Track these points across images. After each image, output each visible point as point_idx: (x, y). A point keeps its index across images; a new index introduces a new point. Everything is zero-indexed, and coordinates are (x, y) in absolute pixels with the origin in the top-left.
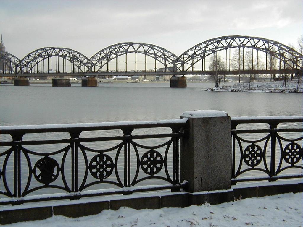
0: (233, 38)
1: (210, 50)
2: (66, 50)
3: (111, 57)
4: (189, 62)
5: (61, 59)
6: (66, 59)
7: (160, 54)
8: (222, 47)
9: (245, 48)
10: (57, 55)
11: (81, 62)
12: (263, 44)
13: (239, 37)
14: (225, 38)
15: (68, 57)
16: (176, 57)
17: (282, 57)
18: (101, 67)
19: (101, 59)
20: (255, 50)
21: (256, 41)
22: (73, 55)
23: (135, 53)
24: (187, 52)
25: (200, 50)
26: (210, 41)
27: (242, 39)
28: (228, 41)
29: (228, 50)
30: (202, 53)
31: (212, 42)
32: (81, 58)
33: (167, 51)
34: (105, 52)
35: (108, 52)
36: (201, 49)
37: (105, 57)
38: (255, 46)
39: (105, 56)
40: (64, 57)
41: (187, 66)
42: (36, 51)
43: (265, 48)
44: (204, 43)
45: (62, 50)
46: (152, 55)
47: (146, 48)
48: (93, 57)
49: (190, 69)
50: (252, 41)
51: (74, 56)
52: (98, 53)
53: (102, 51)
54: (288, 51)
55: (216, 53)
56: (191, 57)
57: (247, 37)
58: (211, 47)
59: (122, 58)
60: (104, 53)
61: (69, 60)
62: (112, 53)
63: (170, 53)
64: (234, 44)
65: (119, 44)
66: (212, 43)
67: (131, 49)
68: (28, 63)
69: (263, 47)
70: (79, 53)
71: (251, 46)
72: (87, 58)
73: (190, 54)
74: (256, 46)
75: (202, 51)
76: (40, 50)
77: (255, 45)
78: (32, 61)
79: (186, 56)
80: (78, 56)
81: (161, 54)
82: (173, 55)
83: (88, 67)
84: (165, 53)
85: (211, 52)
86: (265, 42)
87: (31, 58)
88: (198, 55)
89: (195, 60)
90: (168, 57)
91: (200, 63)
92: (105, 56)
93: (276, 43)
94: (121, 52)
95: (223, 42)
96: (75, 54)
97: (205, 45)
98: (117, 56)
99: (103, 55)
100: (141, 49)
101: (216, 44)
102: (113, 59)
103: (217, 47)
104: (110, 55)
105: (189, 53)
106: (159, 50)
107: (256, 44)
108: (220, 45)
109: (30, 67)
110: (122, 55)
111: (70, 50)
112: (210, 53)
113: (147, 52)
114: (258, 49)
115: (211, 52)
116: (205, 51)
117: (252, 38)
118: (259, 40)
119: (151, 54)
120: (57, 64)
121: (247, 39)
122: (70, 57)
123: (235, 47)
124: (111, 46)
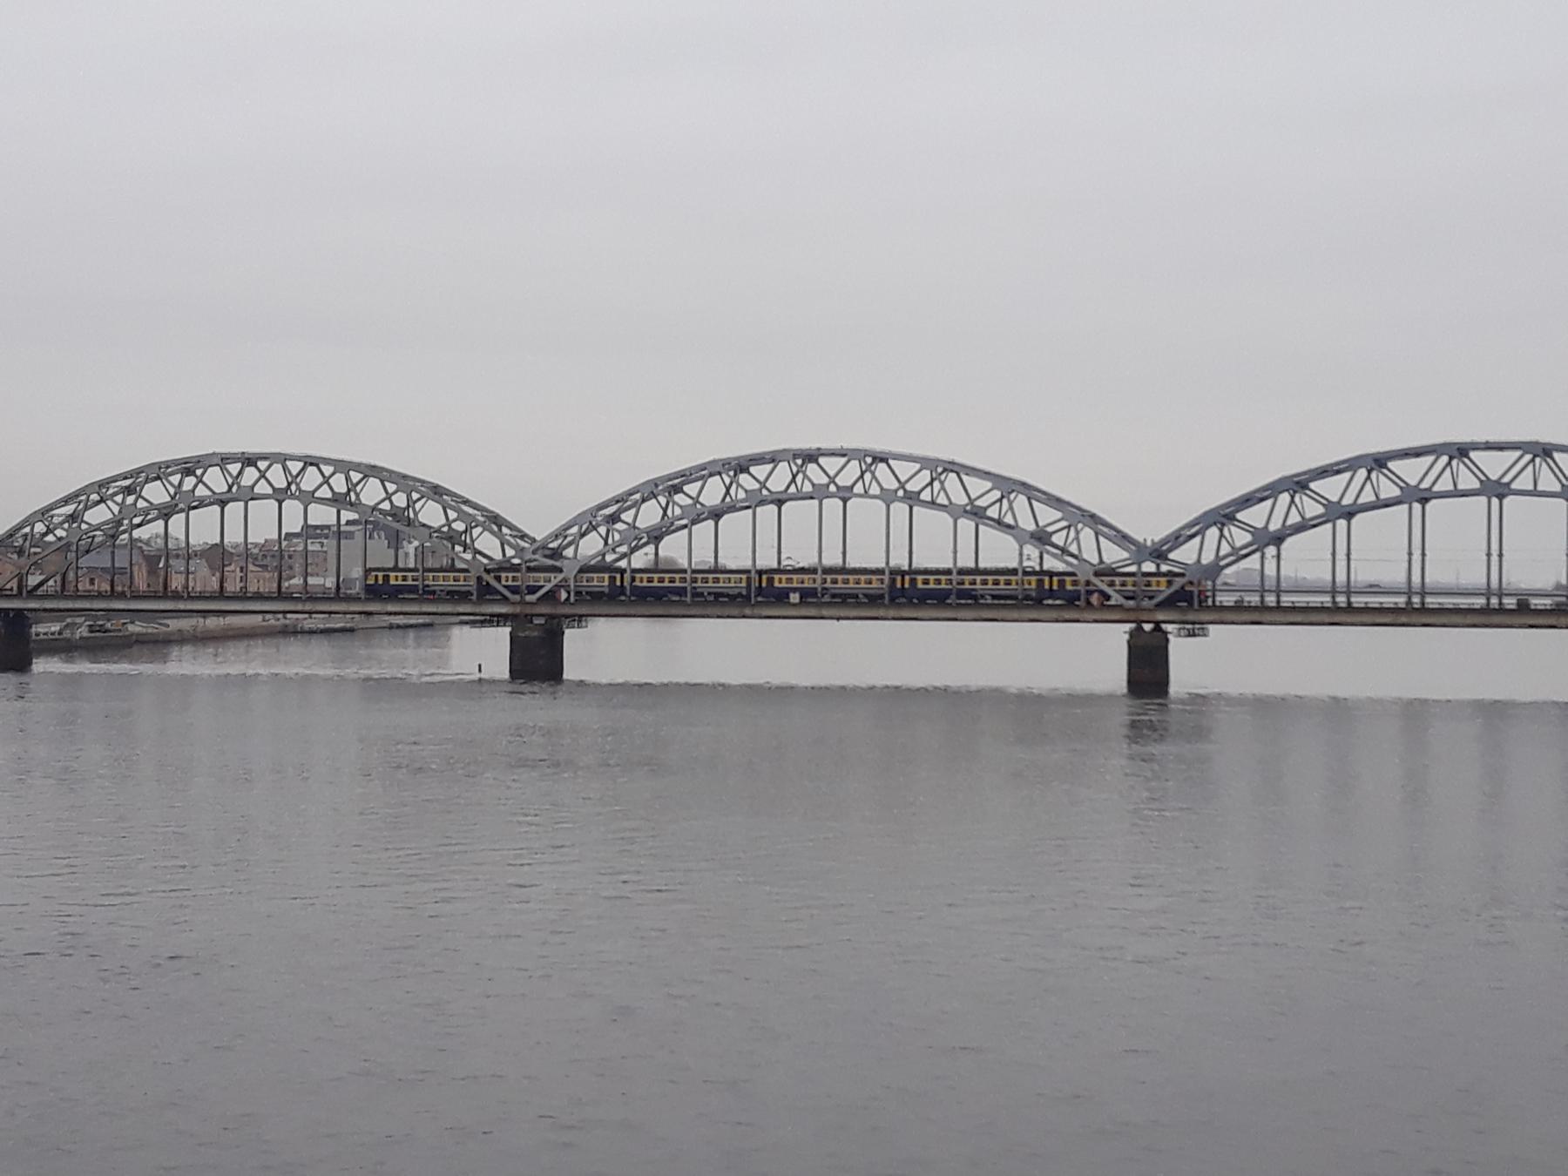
0: (249, 461)
12: (384, 495)
13: (283, 459)
21: (355, 476)
28: (234, 468)
57: (310, 462)
69: (386, 506)
71: (329, 495)
73: (56, 520)
74: (357, 495)
86: (391, 487)
93: (437, 492)
101: (175, 479)
107: (358, 488)
108: (201, 491)
112: (149, 517)
117: (343, 466)
121: (252, 469)
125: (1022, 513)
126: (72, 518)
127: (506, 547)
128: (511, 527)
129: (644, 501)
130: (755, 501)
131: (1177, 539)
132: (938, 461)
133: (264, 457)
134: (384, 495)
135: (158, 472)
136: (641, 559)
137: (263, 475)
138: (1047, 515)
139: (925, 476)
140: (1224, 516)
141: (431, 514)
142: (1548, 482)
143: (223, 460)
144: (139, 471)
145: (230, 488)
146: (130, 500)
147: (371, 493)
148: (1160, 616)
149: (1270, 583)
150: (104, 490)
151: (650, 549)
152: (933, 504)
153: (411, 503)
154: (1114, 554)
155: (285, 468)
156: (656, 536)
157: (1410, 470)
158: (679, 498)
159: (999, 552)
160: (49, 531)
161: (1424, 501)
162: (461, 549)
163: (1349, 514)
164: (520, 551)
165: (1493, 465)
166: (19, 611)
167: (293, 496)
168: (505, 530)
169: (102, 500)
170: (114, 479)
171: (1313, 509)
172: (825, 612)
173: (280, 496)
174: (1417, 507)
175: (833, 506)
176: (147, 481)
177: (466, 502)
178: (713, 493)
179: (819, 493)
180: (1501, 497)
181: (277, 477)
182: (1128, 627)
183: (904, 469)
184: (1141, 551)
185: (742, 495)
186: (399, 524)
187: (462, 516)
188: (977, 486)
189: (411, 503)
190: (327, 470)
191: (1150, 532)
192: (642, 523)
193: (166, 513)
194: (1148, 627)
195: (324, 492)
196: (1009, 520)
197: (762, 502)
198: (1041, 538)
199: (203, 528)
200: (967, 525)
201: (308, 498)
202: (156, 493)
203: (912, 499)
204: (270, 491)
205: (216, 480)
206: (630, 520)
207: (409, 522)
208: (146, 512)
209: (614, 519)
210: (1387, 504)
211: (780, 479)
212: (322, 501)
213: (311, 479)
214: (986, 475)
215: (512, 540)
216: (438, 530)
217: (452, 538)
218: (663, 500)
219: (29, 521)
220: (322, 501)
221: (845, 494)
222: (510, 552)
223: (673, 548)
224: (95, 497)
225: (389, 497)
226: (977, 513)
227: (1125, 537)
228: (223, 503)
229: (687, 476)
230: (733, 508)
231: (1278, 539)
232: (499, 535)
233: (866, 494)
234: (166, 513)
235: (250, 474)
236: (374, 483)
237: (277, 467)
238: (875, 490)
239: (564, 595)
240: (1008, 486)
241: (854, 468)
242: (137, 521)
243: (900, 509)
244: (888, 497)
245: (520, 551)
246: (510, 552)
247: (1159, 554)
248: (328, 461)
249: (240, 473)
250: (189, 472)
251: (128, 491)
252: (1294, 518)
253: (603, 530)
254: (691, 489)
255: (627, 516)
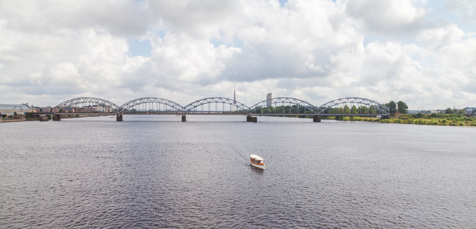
0: (86, 98)
1: (74, 103)
13: (90, 98)
21: (98, 100)
28: (84, 99)
57: (93, 98)
69: (102, 103)
86: (102, 101)
93: (108, 102)
101: (77, 100)
108: (80, 101)
117: (97, 99)
125: (171, 104)
126: (65, 104)
128: (116, 105)
129: (131, 103)
130: (143, 103)
131: (186, 107)
132: (162, 99)
133: (87, 98)
135: (75, 99)
136: (131, 109)
138: (174, 104)
139: (161, 100)
140: (191, 104)
141: (107, 104)
142: (221, 101)
143: (83, 98)
144: (73, 99)
146: (72, 102)
147: (100, 102)
148: (185, 114)
149: (195, 111)
151: (132, 107)
152: (162, 103)
153: (105, 103)
154: (180, 108)
156: (132, 106)
157: (209, 100)
158: (135, 102)
159: (169, 108)
160: (62, 106)
161: (210, 103)
163: (203, 104)
164: (117, 108)
165: (216, 100)
166: (59, 115)
169: (68, 102)
171: (200, 104)
172: (151, 114)
173: (90, 102)
174: (209, 103)
175: (151, 103)
176: (74, 100)
177: (111, 103)
178: (138, 102)
179: (150, 102)
180: (217, 103)
181: (89, 100)
182: (181, 116)
183: (159, 100)
184: (183, 108)
185: (142, 102)
186: (103, 106)
187: (111, 104)
188: (166, 101)
189: (105, 103)
190: (95, 99)
191: (184, 106)
192: (131, 105)
193: (76, 104)
194: (184, 115)
195: (95, 102)
196: (170, 105)
197: (144, 103)
198: (173, 106)
199: (81, 106)
200: (165, 105)
201: (93, 102)
202: (75, 102)
203: (160, 102)
204: (88, 101)
205: (82, 100)
207: (105, 105)
208: (74, 104)
209: (128, 104)
210: (206, 103)
211: (146, 100)
212: (94, 102)
213: (93, 100)
214: (167, 100)
217: (110, 106)
218: (133, 103)
219: (60, 105)
220: (94, 102)
221: (153, 102)
222: (116, 108)
223: (134, 107)
224: (67, 102)
226: (166, 104)
227: (181, 106)
228: (83, 103)
229: (136, 100)
230: (140, 103)
231: (196, 107)
233: (155, 102)
234: (76, 104)
235: (86, 100)
236: (100, 101)
237: (89, 99)
238: (156, 102)
239: (122, 112)
240: (169, 101)
241: (153, 99)
242: (73, 105)
243: (158, 104)
244: (157, 102)
245: (117, 108)
246: (116, 108)
247: (185, 108)
248: (95, 98)
250: (79, 99)
251: (72, 101)
252: (198, 105)
253: (126, 106)
254: (136, 101)
255: (129, 104)
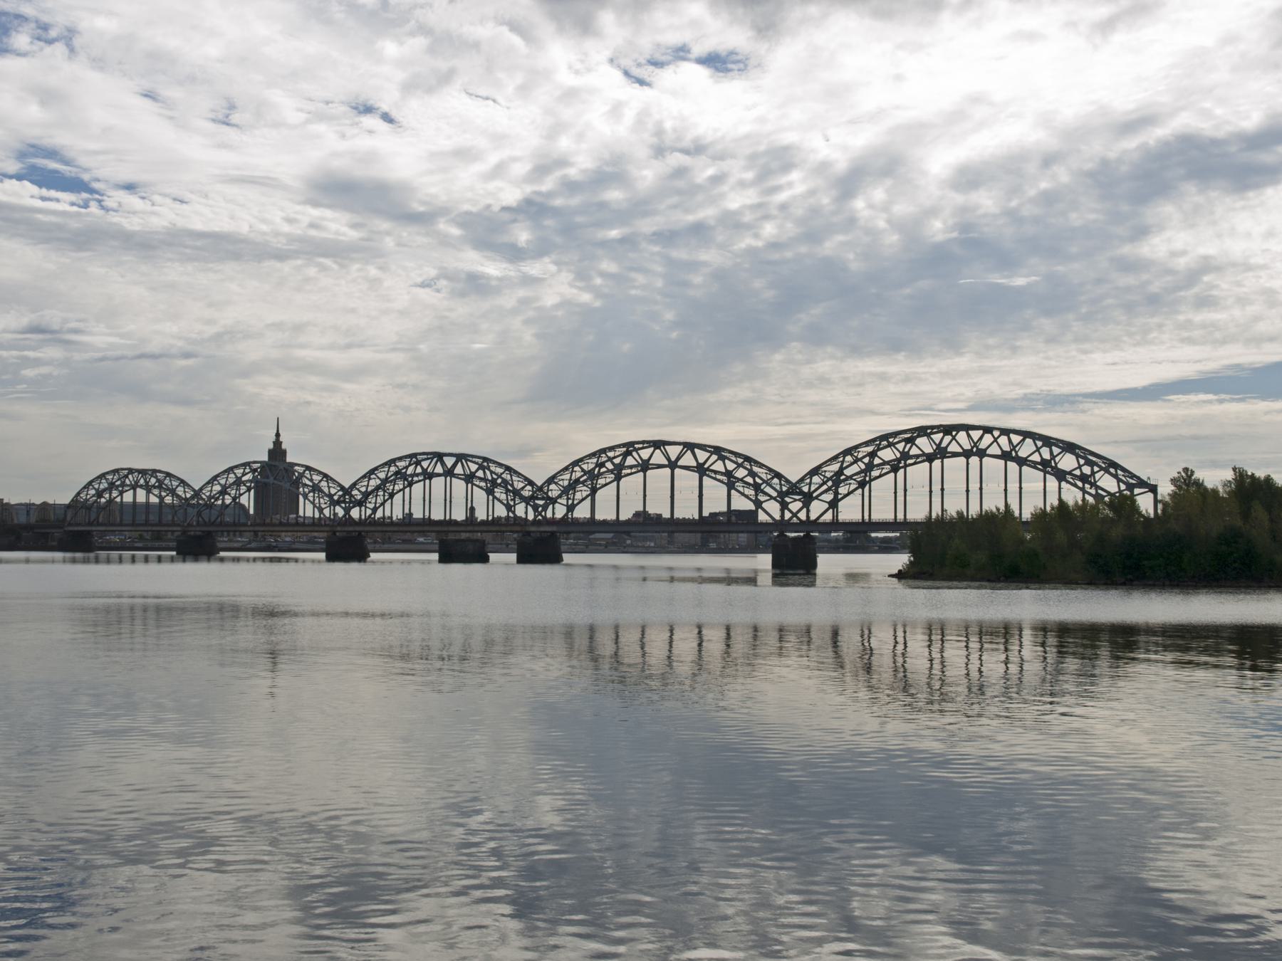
0: (948, 430)
1: (885, 463)
2: (474, 460)
3: (601, 481)
4: (824, 497)
5: (459, 486)
6: (473, 484)
7: (741, 473)
8: (917, 456)
9: (985, 460)
10: (449, 473)
11: (516, 493)
12: (1035, 449)
13: (967, 428)
14: (929, 431)
15: (481, 479)
16: (787, 481)
17: (1087, 486)
18: (571, 508)
19: (573, 485)
20: (1013, 466)
21: (1016, 439)
22: (492, 472)
23: (668, 471)
24: (820, 467)
25: (855, 462)
26: (885, 437)
27: (976, 435)
28: (937, 437)
29: (937, 463)
30: (862, 471)
31: (891, 440)
32: (515, 483)
33: (761, 465)
34: (585, 467)
35: (593, 466)
36: (861, 460)
37: (585, 481)
38: (1014, 454)
39: (585, 477)
40: (469, 478)
41: (817, 508)
42: (392, 462)
43: (1039, 459)
44: (867, 444)
45: (463, 461)
46: (719, 477)
47: (702, 455)
48: (551, 480)
49: (828, 517)
50: (1003, 440)
51: (495, 477)
52: (566, 469)
53: (576, 463)
54: (1107, 471)
55: (902, 471)
56: (830, 483)
58: (887, 454)
59: (632, 483)
60: (583, 470)
61: (481, 488)
62: (603, 470)
63: (770, 470)
64: (954, 448)
65: (624, 445)
66: (890, 445)
67: (658, 458)
68: (366, 495)
69: (1036, 458)
70: (508, 469)
72: (531, 483)
73: (828, 474)
74: (1016, 452)
75: (863, 467)
76: (400, 459)
77: (1011, 450)
78: (378, 488)
79: (816, 479)
80: (507, 476)
81: (746, 472)
82: (778, 475)
83: (535, 508)
84: (756, 469)
85: (887, 468)
86: (1039, 443)
87: (374, 483)
88: (851, 477)
89: (843, 490)
90: (764, 481)
91: (855, 499)
92: (585, 477)
93: (1070, 447)
94: (631, 467)
95: (922, 442)
96: (500, 470)
97: (870, 449)
98: (618, 478)
99: (579, 474)
100: (688, 460)
101: (901, 446)
102: (606, 485)
103: (905, 455)
104: (600, 474)
105: (825, 471)
106: (740, 461)
108: (914, 451)
109: (372, 506)
110: (631, 474)
111: (485, 459)
112: (884, 471)
113: (706, 466)
114: (1022, 462)
115: (887, 468)
116: (870, 467)
117: (1006, 432)
118: (1022, 438)
119: (716, 472)
120: (448, 501)
122: (484, 479)
123: (955, 455)
124: (603, 451)
127: (1121, 484)
134: (1035, 449)
137: (996, 440)
145: (972, 448)
150: (856, 454)
155: (969, 436)
162: (1089, 486)
167: (975, 454)
168: (1119, 472)
170: (856, 447)
195: (994, 450)
205: (924, 444)
206: (1078, 470)
215: (1123, 478)
216: (1070, 473)
225: (1038, 450)
232: (1115, 476)
236: (1029, 441)
249: (981, 438)
250: (907, 441)
